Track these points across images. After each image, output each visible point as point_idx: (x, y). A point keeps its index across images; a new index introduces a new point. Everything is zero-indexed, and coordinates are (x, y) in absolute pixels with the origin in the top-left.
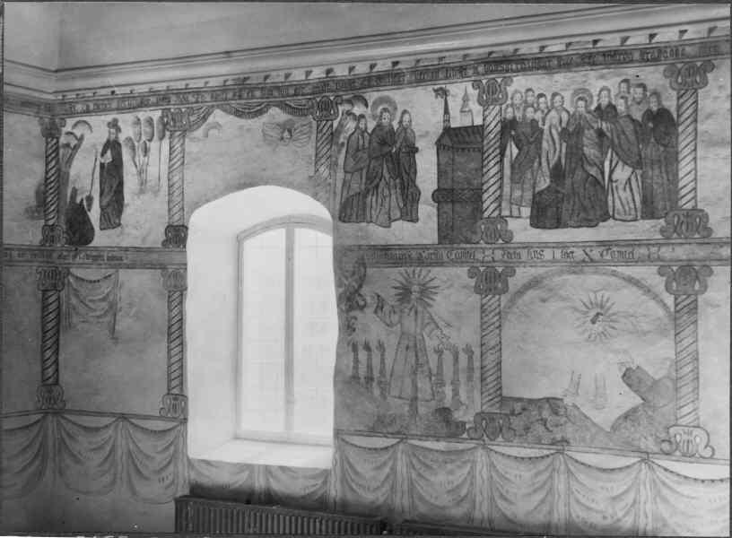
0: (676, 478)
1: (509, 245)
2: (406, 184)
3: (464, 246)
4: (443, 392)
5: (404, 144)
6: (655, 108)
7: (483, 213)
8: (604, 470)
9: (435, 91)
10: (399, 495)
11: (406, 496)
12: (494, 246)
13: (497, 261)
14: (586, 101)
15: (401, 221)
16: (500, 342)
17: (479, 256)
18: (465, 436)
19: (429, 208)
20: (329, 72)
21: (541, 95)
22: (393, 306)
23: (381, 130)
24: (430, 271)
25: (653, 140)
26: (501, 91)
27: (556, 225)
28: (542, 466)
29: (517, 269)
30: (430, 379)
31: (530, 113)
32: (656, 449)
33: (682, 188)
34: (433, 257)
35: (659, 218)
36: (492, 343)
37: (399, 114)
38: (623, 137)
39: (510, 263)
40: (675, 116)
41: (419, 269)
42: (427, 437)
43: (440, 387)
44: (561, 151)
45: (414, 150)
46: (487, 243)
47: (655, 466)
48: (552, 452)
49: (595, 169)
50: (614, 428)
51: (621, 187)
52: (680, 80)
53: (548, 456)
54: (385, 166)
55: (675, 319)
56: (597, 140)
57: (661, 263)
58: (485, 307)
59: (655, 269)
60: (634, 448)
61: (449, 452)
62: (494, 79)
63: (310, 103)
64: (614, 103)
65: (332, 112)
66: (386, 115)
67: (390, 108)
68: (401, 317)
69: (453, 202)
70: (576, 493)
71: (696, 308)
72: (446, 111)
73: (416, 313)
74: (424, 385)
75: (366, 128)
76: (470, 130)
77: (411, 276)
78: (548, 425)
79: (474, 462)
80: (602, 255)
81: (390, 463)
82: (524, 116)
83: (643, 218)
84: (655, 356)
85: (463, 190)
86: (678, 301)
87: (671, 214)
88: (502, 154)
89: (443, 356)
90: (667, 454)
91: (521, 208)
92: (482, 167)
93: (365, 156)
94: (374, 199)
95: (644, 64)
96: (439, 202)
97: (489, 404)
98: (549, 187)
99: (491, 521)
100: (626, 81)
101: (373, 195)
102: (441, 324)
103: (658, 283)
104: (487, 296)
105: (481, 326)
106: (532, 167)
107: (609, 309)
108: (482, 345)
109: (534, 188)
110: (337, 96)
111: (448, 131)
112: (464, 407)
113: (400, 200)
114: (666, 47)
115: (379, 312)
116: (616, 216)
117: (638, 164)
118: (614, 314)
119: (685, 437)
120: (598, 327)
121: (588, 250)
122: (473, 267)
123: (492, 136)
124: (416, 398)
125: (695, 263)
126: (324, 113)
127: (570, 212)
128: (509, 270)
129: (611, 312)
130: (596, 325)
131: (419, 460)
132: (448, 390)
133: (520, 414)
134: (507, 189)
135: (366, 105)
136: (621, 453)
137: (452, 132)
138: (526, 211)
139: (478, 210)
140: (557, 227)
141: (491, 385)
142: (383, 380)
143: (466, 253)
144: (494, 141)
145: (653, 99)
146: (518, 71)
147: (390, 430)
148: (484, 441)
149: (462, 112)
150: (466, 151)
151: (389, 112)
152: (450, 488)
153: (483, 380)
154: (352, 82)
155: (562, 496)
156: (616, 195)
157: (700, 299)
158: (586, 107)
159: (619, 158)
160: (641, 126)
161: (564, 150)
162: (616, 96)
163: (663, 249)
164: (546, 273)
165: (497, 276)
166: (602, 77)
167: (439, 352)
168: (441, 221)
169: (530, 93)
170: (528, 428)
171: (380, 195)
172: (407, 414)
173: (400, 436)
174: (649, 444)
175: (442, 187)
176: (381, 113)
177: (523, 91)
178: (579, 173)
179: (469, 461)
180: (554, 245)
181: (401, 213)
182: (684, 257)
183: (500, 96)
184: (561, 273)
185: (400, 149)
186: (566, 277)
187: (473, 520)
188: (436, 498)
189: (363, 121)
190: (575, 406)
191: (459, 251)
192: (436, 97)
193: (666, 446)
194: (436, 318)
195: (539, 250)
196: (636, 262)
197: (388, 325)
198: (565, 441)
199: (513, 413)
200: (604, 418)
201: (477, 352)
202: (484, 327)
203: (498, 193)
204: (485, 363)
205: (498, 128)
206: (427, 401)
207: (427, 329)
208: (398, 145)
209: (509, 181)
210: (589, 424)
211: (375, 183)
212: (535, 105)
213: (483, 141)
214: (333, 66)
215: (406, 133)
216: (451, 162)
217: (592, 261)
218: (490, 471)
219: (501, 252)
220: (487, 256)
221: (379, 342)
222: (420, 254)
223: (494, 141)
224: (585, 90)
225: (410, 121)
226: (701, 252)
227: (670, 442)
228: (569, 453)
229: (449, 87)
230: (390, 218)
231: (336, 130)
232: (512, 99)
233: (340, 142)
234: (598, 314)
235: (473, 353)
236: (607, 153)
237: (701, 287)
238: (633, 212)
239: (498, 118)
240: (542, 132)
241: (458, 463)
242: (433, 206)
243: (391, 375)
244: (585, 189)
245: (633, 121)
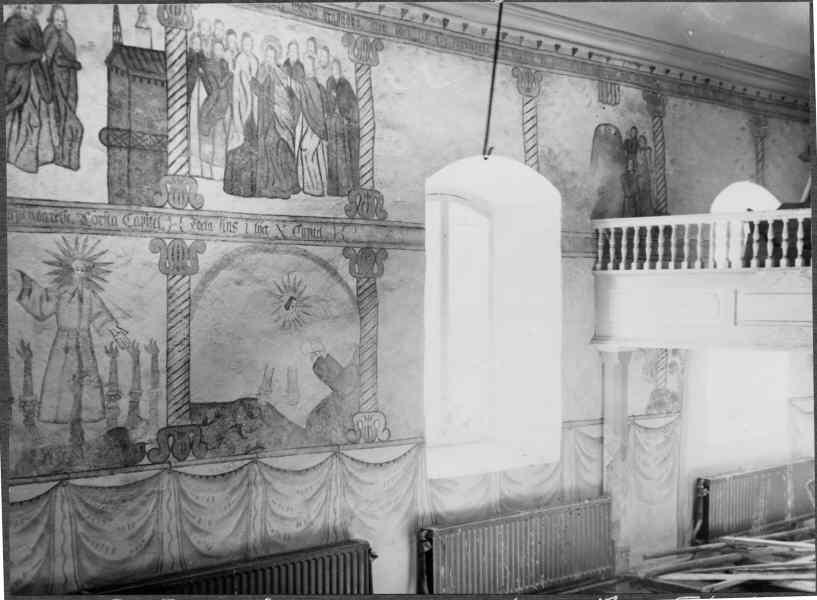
0: (360, 467)
1: (199, 213)
2: (63, 113)
3: (144, 209)
4: (117, 407)
5: (59, 54)
6: (337, 77)
7: (168, 167)
8: (299, 472)
10: (60, 560)
11: (70, 561)
12: (181, 212)
14: (276, 51)
15: (53, 165)
16: (189, 336)
17: (165, 224)
18: (146, 461)
20: (745, 90)
21: (230, 32)
22: (46, 289)
23: (20, 24)
24: (99, 241)
25: (337, 111)
26: (185, 13)
27: (251, 193)
28: (236, 480)
29: (208, 244)
30: (102, 391)
31: (219, 51)
32: (344, 440)
33: (363, 166)
34: (103, 221)
35: (342, 196)
36: (180, 337)
38: (310, 101)
39: (201, 235)
40: (354, 88)
41: (84, 236)
42: (96, 471)
43: (114, 401)
44: (252, 105)
45: (76, 65)
46: (174, 208)
47: (345, 458)
48: (246, 462)
49: (287, 132)
50: (309, 423)
51: (309, 158)
52: (356, 52)
53: (241, 468)
54: (33, 80)
55: (359, 303)
56: (288, 99)
57: (345, 244)
58: (172, 292)
59: (340, 250)
60: (327, 443)
61: (127, 486)
64: (302, 60)
68: (58, 305)
69: (129, 148)
70: (272, 504)
71: (375, 291)
73: (81, 300)
74: (92, 399)
76: (148, 55)
77: (73, 246)
78: (243, 433)
79: (160, 493)
80: (294, 232)
81: (45, 520)
82: (212, 53)
83: (329, 194)
84: (339, 341)
85: (144, 134)
86: (360, 284)
87: (353, 193)
88: (189, 94)
89: (118, 359)
90: (354, 443)
91: (214, 169)
92: (168, 108)
94: (15, 127)
95: (324, 24)
96: (109, 146)
97: (176, 415)
98: (243, 145)
99: (182, 563)
100: (312, 39)
101: (13, 121)
102: (117, 314)
103: (343, 265)
105: (168, 314)
106: (223, 118)
107: (301, 293)
108: (169, 340)
109: (227, 147)
110: (376, 39)
111: (118, 47)
112: (144, 424)
113: (55, 131)
114: (344, 13)
115: (25, 300)
116: (306, 190)
117: (324, 136)
118: (305, 299)
119: (366, 424)
120: (291, 314)
121: (281, 226)
122: (157, 238)
124: (78, 421)
125: (375, 246)
127: (265, 179)
128: (199, 244)
129: (304, 295)
131: (87, 505)
132: (124, 403)
133: (211, 423)
134: (194, 140)
136: (315, 449)
137: (124, 51)
138: (219, 172)
139: (161, 165)
140: (252, 196)
141: (177, 391)
142: (29, 399)
143: (147, 218)
145: (335, 66)
147: (43, 470)
148: (170, 463)
150: (145, 82)
152: (129, 533)
155: (259, 513)
156: (305, 167)
157: (378, 281)
158: (275, 58)
159: (309, 125)
160: (325, 92)
161: (256, 104)
162: (304, 54)
163: (347, 229)
164: (238, 250)
165: (186, 251)
166: (292, 28)
167: (112, 352)
168: (112, 172)
169: (219, 25)
170: (222, 439)
171: (24, 123)
172: (67, 443)
173: (58, 477)
174: (337, 436)
175: (114, 125)
177: (213, 20)
178: (271, 133)
179: (153, 492)
180: (248, 217)
181: (55, 155)
182: (364, 239)
183: (185, 19)
184: (254, 250)
185: (53, 59)
186: (259, 255)
187: (162, 566)
188: (114, 551)
190: (268, 405)
191: (140, 216)
193: (351, 436)
194: (109, 305)
195: (233, 221)
196: (325, 241)
197: (36, 318)
198: (260, 447)
199: (205, 423)
200: (297, 412)
201: (163, 349)
202: (171, 316)
203: (185, 144)
204: (171, 363)
205: (183, 60)
206: (95, 421)
207: (98, 321)
208: (50, 52)
210: (285, 423)
211: (16, 102)
212: (224, 42)
214: (671, 68)
215: (60, 36)
216: (127, 93)
217: (285, 238)
218: (179, 500)
221: (22, 342)
222: (84, 217)
224: (276, 40)
225: (65, 21)
226: (379, 235)
227: (353, 430)
228: (263, 460)
230: (37, 158)
232: (199, 26)
234: (292, 298)
235: (158, 351)
236: (298, 116)
237: (378, 269)
238: (320, 187)
239: (183, 47)
240: (232, 77)
241: (142, 498)
242: (103, 151)
243: (42, 392)
244: (277, 154)
245: (319, 86)
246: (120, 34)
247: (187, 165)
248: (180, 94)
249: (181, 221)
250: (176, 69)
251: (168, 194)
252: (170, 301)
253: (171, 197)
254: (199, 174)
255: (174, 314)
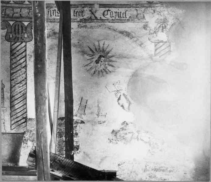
13: (23, 17)
16: (26, 78)
36: (20, 79)
80: (103, 15)
104: (16, 43)
105: (11, 66)
130: (99, 65)
141: (18, 111)
153: (12, 106)
219: (27, 11)
220: (17, 13)
234: (100, 57)
249: (21, 11)
252: (13, 57)
255: (15, 65)
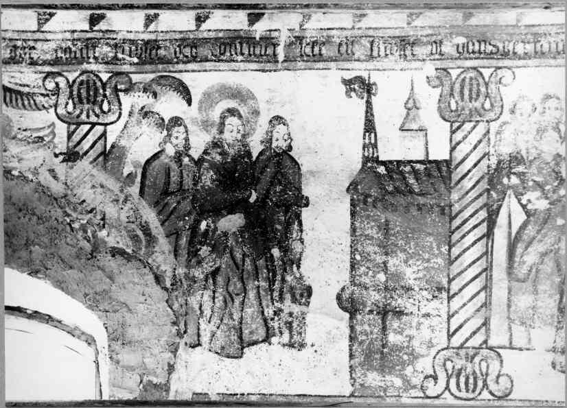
9: (348, 83)
19: (330, 323)
26: (487, 96)
37: (263, 121)
62: (475, 68)
63: (51, 85)
65: (105, 107)
66: (232, 121)
67: (243, 110)
72: (370, 127)
75: (187, 147)
88: (491, 222)
93: (186, 205)
123: (470, 185)
126: (87, 106)
135: (189, 102)
144: (472, 194)
146: (526, 56)
149: (402, 129)
151: (240, 117)
154: (152, 45)
176: (223, 118)
183: (487, 106)
189: (178, 132)
192: (348, 94)
209: (504, 275)
213: (449, 189)
223: (472, 194)
229: (375, 78)
230: (241, 338)
231: (113, 147)
233: (125, 174)
246: (375, 146)
247: (483, 330)
248: (473, 222)
250: (467, 184)
251: (449, 377)
253: (453, 381)
254: (508, 345)
